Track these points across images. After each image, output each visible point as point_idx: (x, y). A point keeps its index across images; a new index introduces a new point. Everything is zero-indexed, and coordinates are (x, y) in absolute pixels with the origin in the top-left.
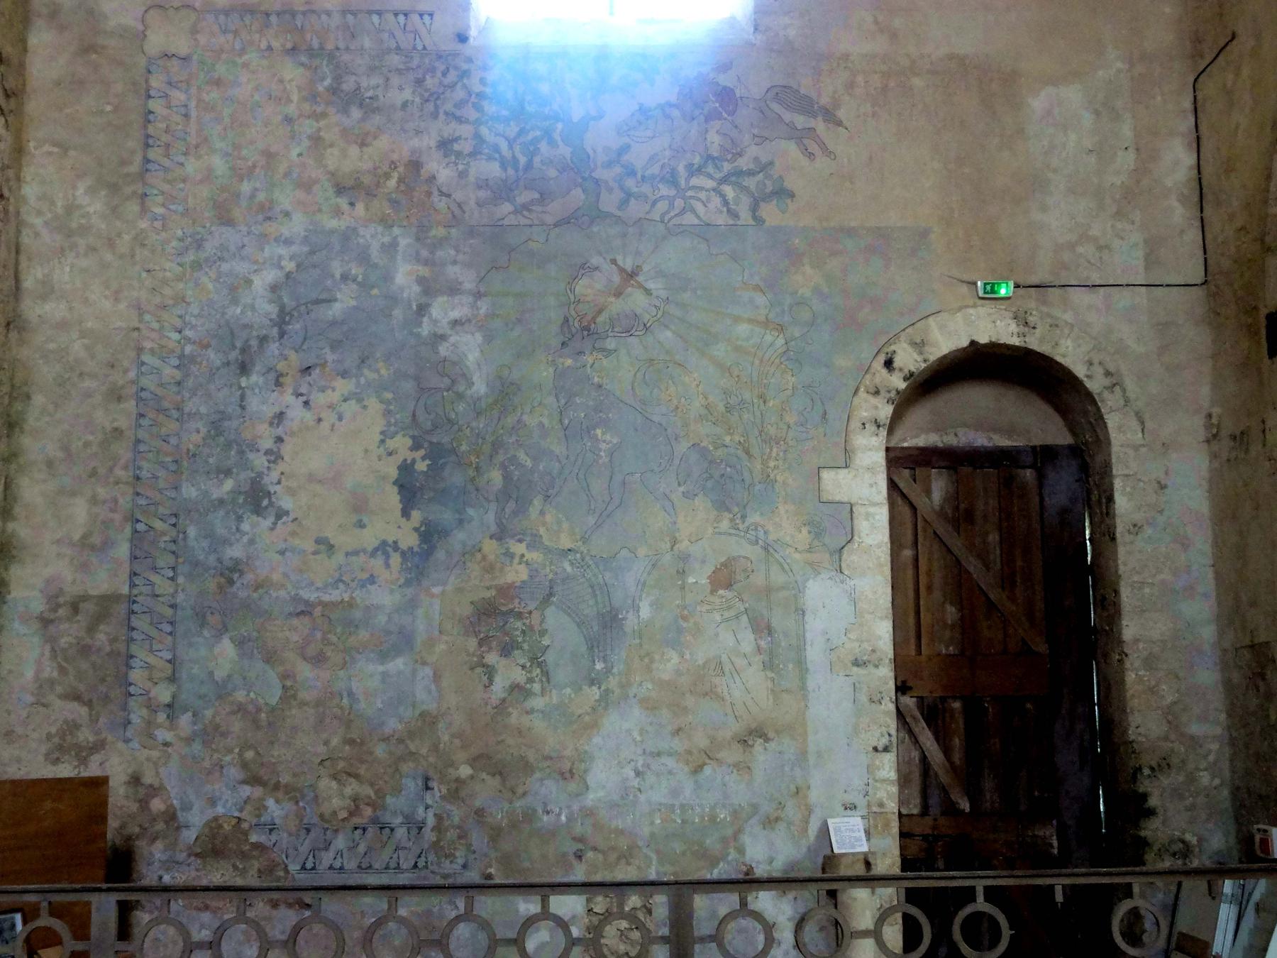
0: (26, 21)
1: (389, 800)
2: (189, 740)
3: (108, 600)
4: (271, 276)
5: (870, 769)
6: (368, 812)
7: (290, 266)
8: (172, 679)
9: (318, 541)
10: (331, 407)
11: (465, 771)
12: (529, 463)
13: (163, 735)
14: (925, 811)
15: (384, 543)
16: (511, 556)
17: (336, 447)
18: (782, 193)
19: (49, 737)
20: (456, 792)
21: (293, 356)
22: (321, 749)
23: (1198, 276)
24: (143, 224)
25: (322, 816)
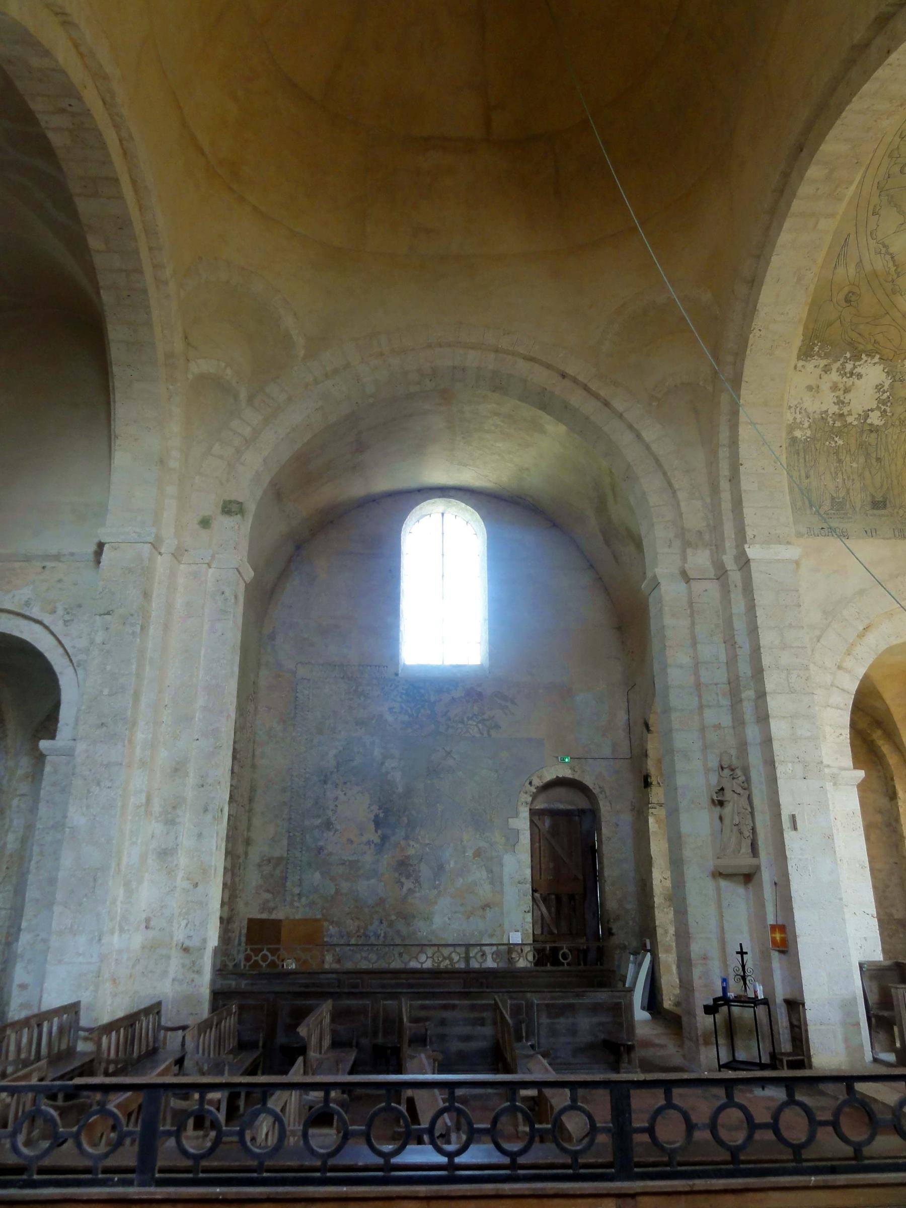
2: (304, 906)
3: (280, 859)
4: (334, 752)
5: (524, 919)
6: (362, 931)
8: (300, 886)
9: (348, 840)
11: (393, 917)
13: (296, 904)
14: (542, 933)
16: (409, 845)
17: (355, 807)
18: (497, 727)
20: (391, 924)
23: (629, 756)
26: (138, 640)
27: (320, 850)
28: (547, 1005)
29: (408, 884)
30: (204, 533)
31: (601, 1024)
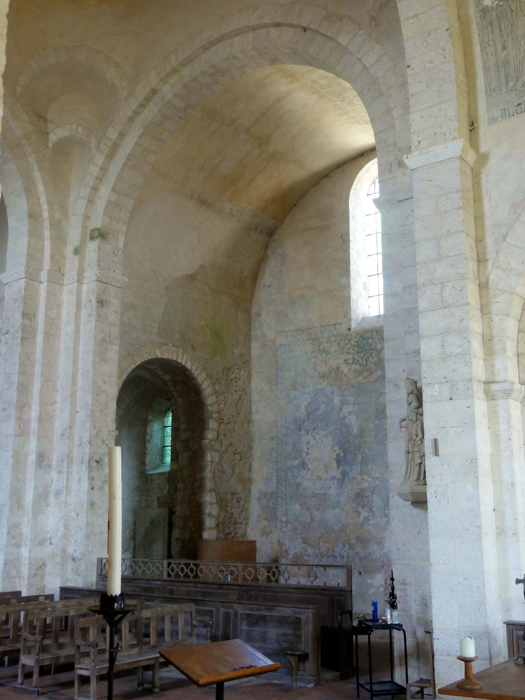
0: (250, 341)
1: (336, 549)
3: (272, 493)
6: (331, 552)
7: (309, 400)
8: (286, 515)
9: (318, 477)
10: (320, 439)
11: (354, 541)
12: (368, 452)
13: (284, 529)
15: (333, 477)
16: (364, 479)
17: (321, 449)
19: (261, 530)
21: (311, 425)
22: (319, 534)
24: (277, 392)
25: (320, 553)
26: (20, 348)
27: (299, 485)
28: (248, 615)
29: (364, 513)
30: (76, 259)
31: (285, 635)
